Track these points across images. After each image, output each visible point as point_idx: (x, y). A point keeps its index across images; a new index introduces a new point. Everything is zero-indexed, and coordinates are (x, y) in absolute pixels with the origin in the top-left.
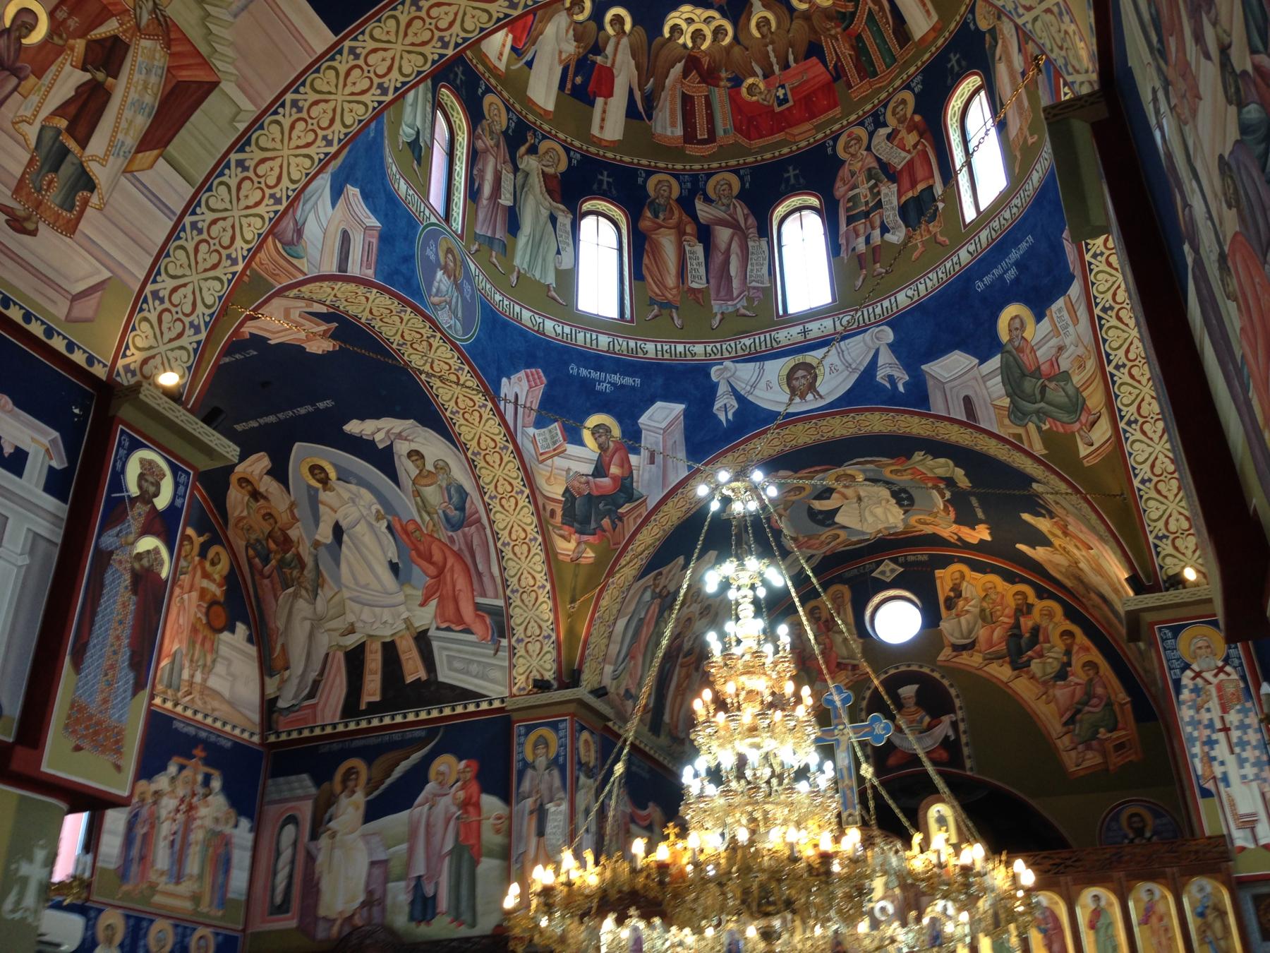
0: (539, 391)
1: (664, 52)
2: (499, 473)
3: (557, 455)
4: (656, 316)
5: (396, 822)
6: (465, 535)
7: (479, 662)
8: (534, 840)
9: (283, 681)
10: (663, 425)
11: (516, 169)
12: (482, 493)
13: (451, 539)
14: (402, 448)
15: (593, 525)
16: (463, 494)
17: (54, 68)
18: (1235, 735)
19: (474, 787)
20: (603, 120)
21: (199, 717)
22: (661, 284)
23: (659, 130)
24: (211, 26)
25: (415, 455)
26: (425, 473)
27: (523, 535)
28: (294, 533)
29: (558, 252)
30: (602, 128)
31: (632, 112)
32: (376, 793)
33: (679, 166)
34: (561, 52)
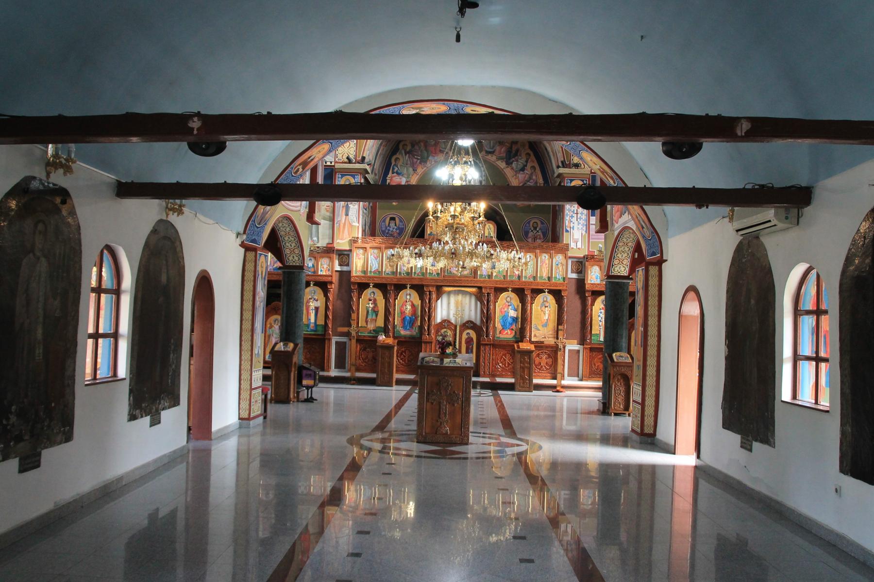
8: (344, 217)
18: (579, 215)
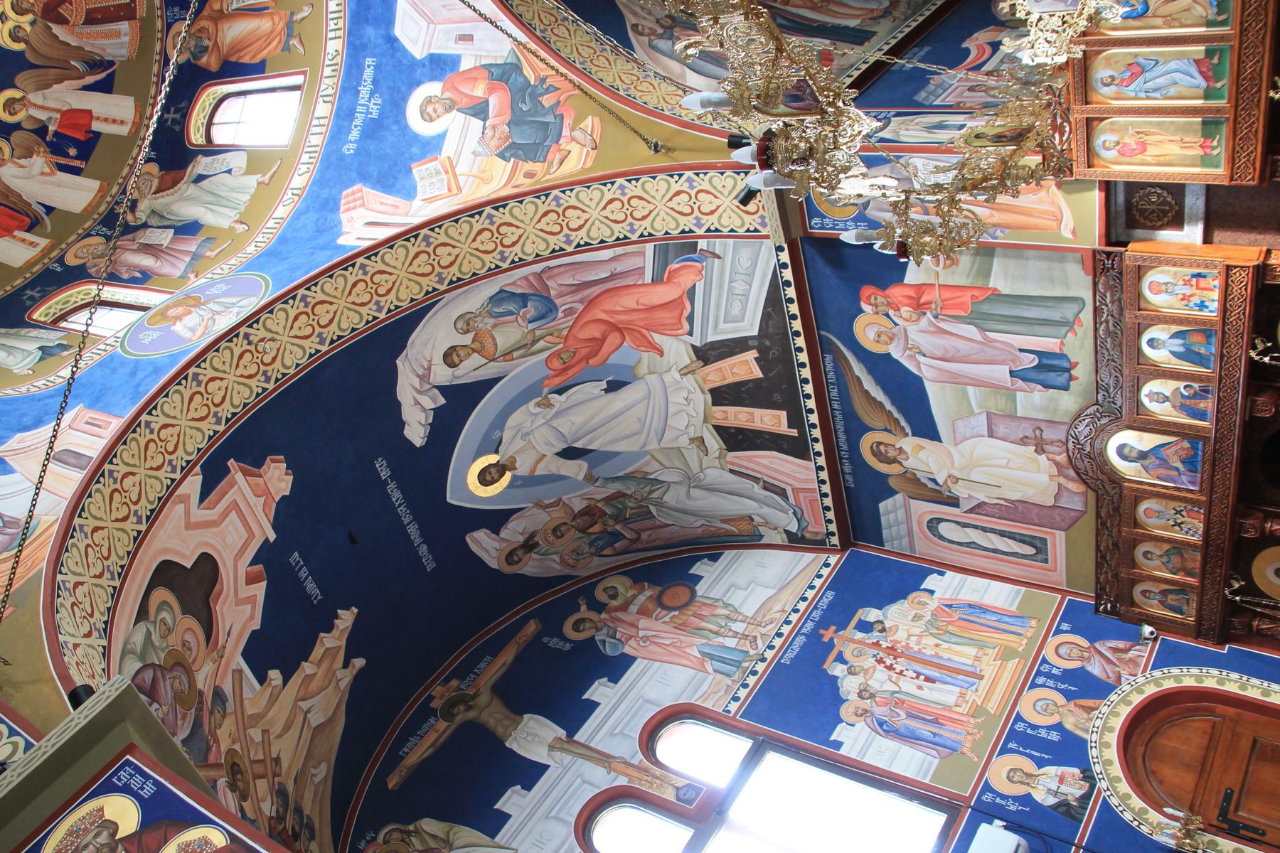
0: (371, 195)
1: (44, 50)
2: (465, 248)
3: (453, 169)
4: (301, 42)
5: (939, 400)
6: (561, 295)
7: (730, 282)
9: (766, 523)
10: (424, 24)
11: (145, 226)
12: (496, 271)
13: (568, 312)
14: (442, 375)
15: (550, 119)
16: (501, 297)
19: (895, 292)
20: (114, 121)
21: (786, 630)
22: (269, 37)
23: (124, 52)
25: (450, 357)
26: (476, 346)
27: (553, 216)
28: (578, 505)
29: (229, 172)
30: (122, 122)
31: (105, 87)
32: (903, 423)
33: (159, 24)
34: (43, 174)
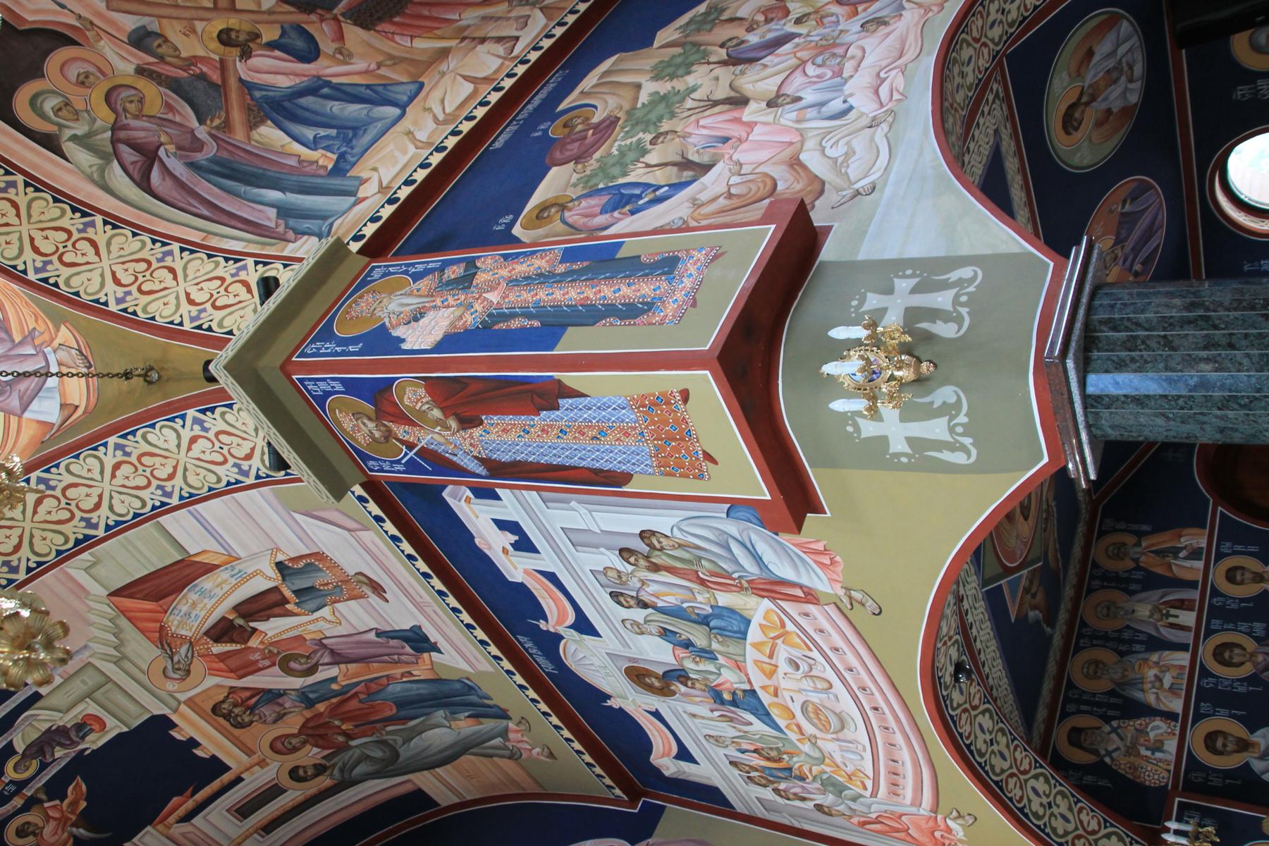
17: (284, 637)
24: (114, 639)
